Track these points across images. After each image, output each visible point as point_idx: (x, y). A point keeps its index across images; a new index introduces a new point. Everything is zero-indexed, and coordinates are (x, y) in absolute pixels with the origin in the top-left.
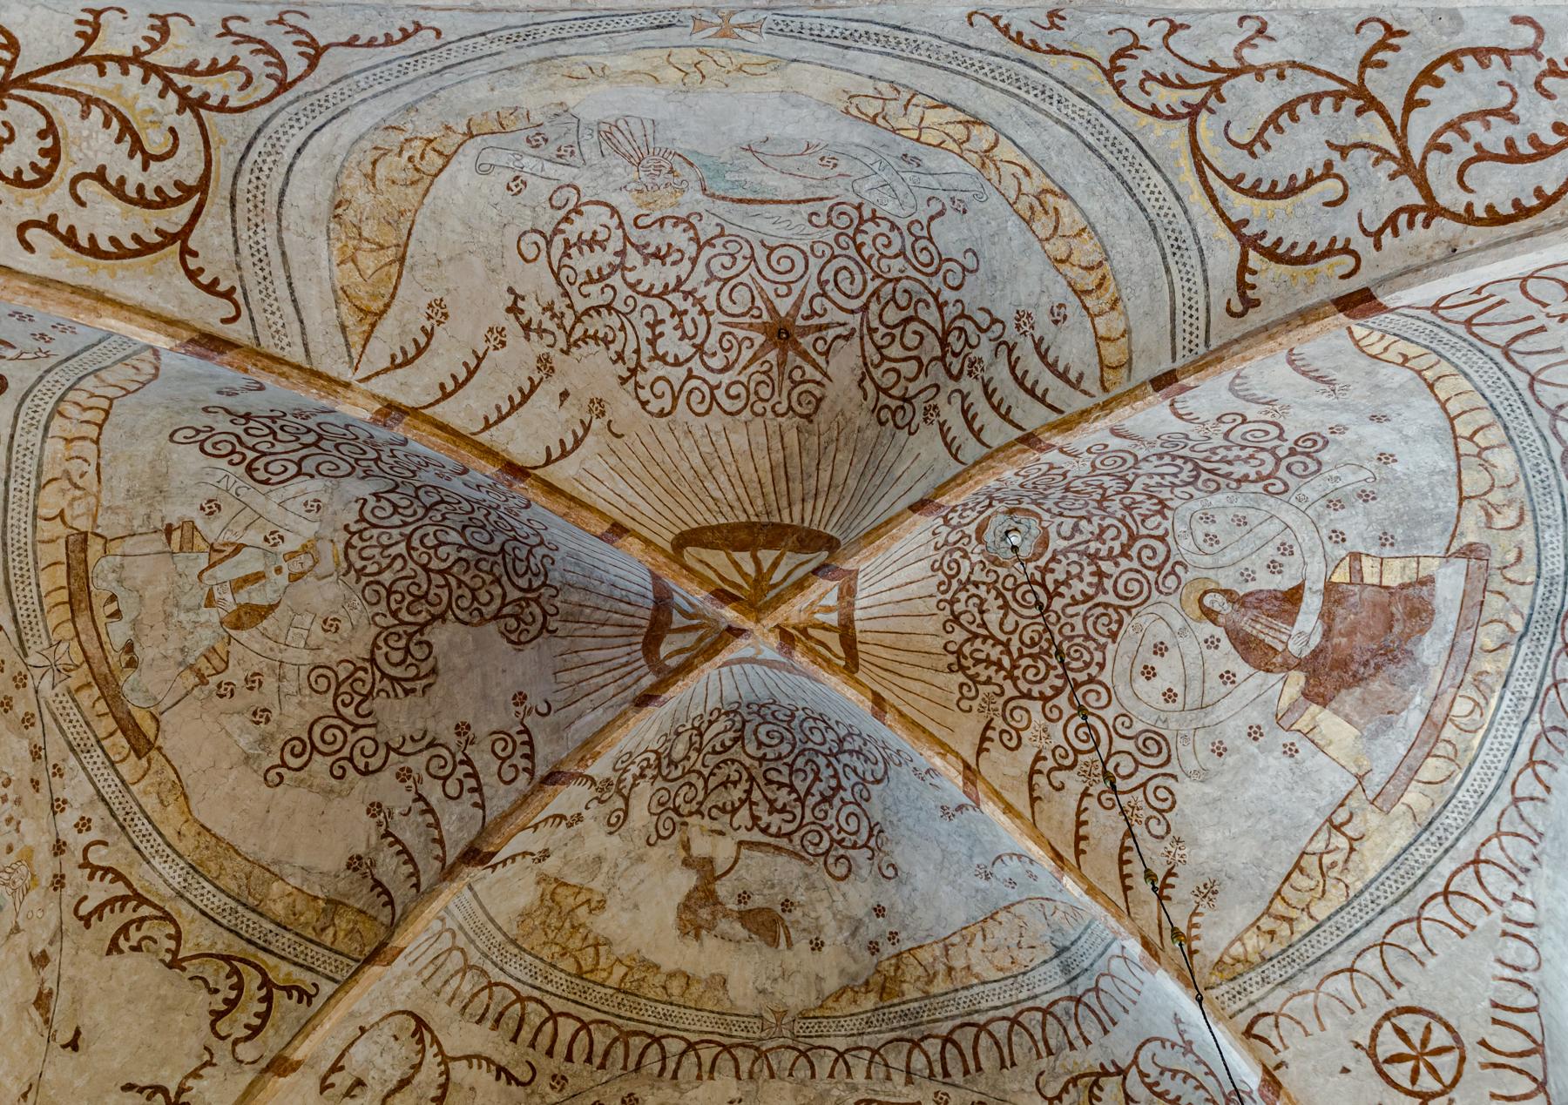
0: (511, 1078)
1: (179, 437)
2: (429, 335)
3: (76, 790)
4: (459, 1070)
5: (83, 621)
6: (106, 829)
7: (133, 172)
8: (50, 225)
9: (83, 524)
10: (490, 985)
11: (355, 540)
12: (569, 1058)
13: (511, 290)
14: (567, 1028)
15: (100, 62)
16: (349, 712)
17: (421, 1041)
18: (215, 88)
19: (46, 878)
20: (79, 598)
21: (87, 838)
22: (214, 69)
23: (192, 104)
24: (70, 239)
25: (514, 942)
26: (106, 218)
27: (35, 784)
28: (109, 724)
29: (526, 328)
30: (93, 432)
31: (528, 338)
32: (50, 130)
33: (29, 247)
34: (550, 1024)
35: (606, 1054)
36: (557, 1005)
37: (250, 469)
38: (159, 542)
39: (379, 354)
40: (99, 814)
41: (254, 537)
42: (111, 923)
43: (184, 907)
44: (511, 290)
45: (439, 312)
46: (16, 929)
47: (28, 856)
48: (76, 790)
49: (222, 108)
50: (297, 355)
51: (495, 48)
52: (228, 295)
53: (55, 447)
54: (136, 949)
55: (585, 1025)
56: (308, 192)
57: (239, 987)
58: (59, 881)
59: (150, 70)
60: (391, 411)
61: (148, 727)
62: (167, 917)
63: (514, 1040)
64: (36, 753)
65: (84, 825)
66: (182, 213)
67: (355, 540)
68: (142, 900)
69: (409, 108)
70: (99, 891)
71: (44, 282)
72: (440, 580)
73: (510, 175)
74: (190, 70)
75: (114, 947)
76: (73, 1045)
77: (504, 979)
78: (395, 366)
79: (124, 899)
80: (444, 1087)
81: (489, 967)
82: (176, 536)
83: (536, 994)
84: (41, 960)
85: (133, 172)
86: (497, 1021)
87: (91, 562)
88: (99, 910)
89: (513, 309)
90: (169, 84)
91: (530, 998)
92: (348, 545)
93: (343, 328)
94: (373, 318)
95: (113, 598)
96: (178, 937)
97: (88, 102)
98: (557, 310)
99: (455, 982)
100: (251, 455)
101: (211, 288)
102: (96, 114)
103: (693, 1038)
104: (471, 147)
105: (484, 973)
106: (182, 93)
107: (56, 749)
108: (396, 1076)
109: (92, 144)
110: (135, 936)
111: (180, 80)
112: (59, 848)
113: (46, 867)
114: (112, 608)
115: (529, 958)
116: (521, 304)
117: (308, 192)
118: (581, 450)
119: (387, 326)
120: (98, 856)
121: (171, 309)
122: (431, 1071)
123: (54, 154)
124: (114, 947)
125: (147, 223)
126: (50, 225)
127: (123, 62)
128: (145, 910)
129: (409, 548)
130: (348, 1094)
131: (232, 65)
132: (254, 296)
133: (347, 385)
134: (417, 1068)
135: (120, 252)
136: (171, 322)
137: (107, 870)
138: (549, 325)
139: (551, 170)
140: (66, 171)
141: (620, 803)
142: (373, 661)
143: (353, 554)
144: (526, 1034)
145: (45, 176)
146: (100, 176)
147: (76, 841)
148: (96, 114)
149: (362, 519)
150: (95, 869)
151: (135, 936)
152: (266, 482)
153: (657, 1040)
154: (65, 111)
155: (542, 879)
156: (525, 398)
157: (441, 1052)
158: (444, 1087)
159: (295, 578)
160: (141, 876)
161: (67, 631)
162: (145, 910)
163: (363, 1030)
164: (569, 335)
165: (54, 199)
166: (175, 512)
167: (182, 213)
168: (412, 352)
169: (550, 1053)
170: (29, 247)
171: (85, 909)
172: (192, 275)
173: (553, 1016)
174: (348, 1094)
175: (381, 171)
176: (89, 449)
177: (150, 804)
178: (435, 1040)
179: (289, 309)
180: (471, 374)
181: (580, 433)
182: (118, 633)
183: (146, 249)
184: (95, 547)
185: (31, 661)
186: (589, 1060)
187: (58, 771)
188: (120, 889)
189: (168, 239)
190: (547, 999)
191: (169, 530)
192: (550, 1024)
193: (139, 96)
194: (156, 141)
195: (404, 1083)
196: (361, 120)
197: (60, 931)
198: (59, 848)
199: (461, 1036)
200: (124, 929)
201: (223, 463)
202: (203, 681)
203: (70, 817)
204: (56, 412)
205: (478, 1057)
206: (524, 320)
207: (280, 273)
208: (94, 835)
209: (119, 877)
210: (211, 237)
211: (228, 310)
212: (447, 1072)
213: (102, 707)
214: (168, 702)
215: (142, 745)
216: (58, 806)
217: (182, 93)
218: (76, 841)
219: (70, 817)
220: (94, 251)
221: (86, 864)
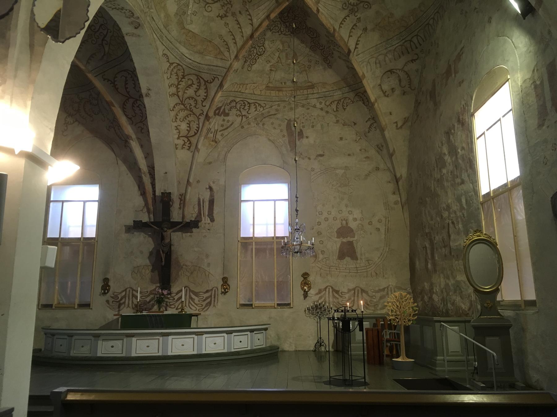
0: (415, 60)
1: (249, 69)
2: (225, 41)
3: (314, 102)
4: (406, 69)
5: (284, 89)
6: (324, 100)
7: (195, 86)
8: (203, 102)
9: (264, 87)
10: (394, 50)
11: (283, 33)
12: (420, 45)
13: (217, 17)
14: (415, 40)
15: (178, 92)
16: (321, 48)
17: (394, 72)
18: (180, 74)
19: (324, 114)
20: (279, 89)
21: (323, 104)
22: (177, 75)
23: (184, 77)
24: (205, 99)
25: (388, 40)
26: (202, 92)
27: (308, 109)
28: (305, 92)
29: (226, 16)
30: (245, 86)
31: (227, 16)
32: (189, 98)
33: (205, 106)
34: (412, 43)
35: (425, 37)
36: (409, 38)
37: (261, 55)
38: (274, 73)
39: (226, 54)
40: (321, 100)
41: (277, 54)
42: (340, 106)
43: (345, 94)
44: (217, 17)
45: (221, 36)
46: (328, 124)
47: (318, 115)
48: (314, 102)
49: (184, 72)
50: (225, 70)
51: (165, 38)
52: (215, 78)
53: (247, 91)
54: (347, 106)
55: (417, 35)
56: (197, 58)
57: (361, 97)
58: (327, 112)
59: (178, 84)
60: (236, 57)
61: (310, 84)
62: (345, 98)
63: (409, 53)
64: (303, 106)
65: (321, 103)
66: (202, 80)
67: (283, 33)
68: (340, 100)
69: (180, 43)
70: (334, 106)
71: (210, 107)
72: (296, 18)
73: (193, 16)
74: (178, 79)
75: (345, 109)
76: (355, 124)
77: (395, 47)
78: (229, 51)
79: (338, 103)
80: (407, 74)
81: (390, 49)
82: (273, 69)
83: (404, 41)
84: (337, 121)
85: (195, 86)
86: (403, 54)
87: (272, 86)
88: (337, 108)
89: (222, 17)
90: (181, 81)
91: (403, 43)
92: (285, 34)
93: (221, 59)
94: (221, 52)
95: (282, 83)
96: (349, 99)
97: (184, 93)
98: (223, 4)
99: (387, 59)
100: (257, 55)
101: (213, 80)
102: (186, 91)
103: (432, 17)
104: (187, 27)
105: (390, 51)
106: (182, 79)
107: (304, 102)
108: (397, 81)
109: (190, 92)
110: (345, 105)
111: (180, 79)
112: (322, 109)
113: (324, 113)
114: (283, 84)
115: (395, 38)
116: (220, 15)
117: (197, 58)
118: (252, 14)
119: (222, 49)
120: (328, 103)
121: (216, 88)
122: (402, 74)
123: (192, 98)
124: (345, 109)
125: (203, 87)
126: (203, 102)
127: (177, 89)
128: (342, 100)
129: (288, 22)
130: (393, 92)
131: (176, 73)
132: (215, 73)
133: (231, 64)
134: (399, 76)
135: (207, 92)
136: (218, 89)
137: (331, 103)
138: (225, 8)
139: (190, 6)
140: (195, 97)
141: (362, 5)
142: (312, 38)
143: (287, 34)
144: (410, 50)
145: (196, 100)
146: (196, 92)
147: (323, 106)
148: (186, 91)
149: (278, 32)
150: (330, 105)
151: (345, 105)
152: (264, 52)
153: (428, 24)
154: (186, 96)
155: (373, 30)
156: (239, 24)
157: (399, 70)
158: (407, 74)
159: (289, 47)
160: (336, 98)
161: (284, 93)
162: (342, 100)
163: (380, 85)
164: (228, 3)
165: (199, 99)
166: (267, 68)
167: (202, 80)
168: (227, 46)
169: (417, 48)
170: (205, 106)
171: (335, 110)
172: (211, 83)
173: (411, 41)
174: (393, 92)
175: (193, 44)
176: (249, 85)
177: (324, 90)
178: (396, 69)
179: (217, 68)
180: (233, 35)
181: (248, 13)
182: (289, 84)
183: (206, 89)
184: (270, 85)
185: (287, 100)
186: (424, 41)
187: (309, 103)
188: (336, 102)
189: (205, 84)
190: (407, 39)
191: (271, 70)
192: (412, 43)
193: (183, 84)
194: (190, 82)
195: (400, 81)
196: (184, 50)
197: (336, 116)
198: (322, 109)
199: (400, 64)
200: (343, 106)
201: (258, 60)
202: (306, 71)
203: (318, 105)
204: (240, 92)
205: (406, 63)
206: (224, 16)
207: (212, 67)
208: (324, 102)
209: (333, 102)
210: (206, 77)
211: (216, 79)
212: (405, 71)
213: (301, 91)
214: (307, 79)
215: (312, 87)
216: (315, 106)
217: (182, 79)
218: (323, 106)
219: (318, 105)
220: (206, 96)
221: (328, 106)
